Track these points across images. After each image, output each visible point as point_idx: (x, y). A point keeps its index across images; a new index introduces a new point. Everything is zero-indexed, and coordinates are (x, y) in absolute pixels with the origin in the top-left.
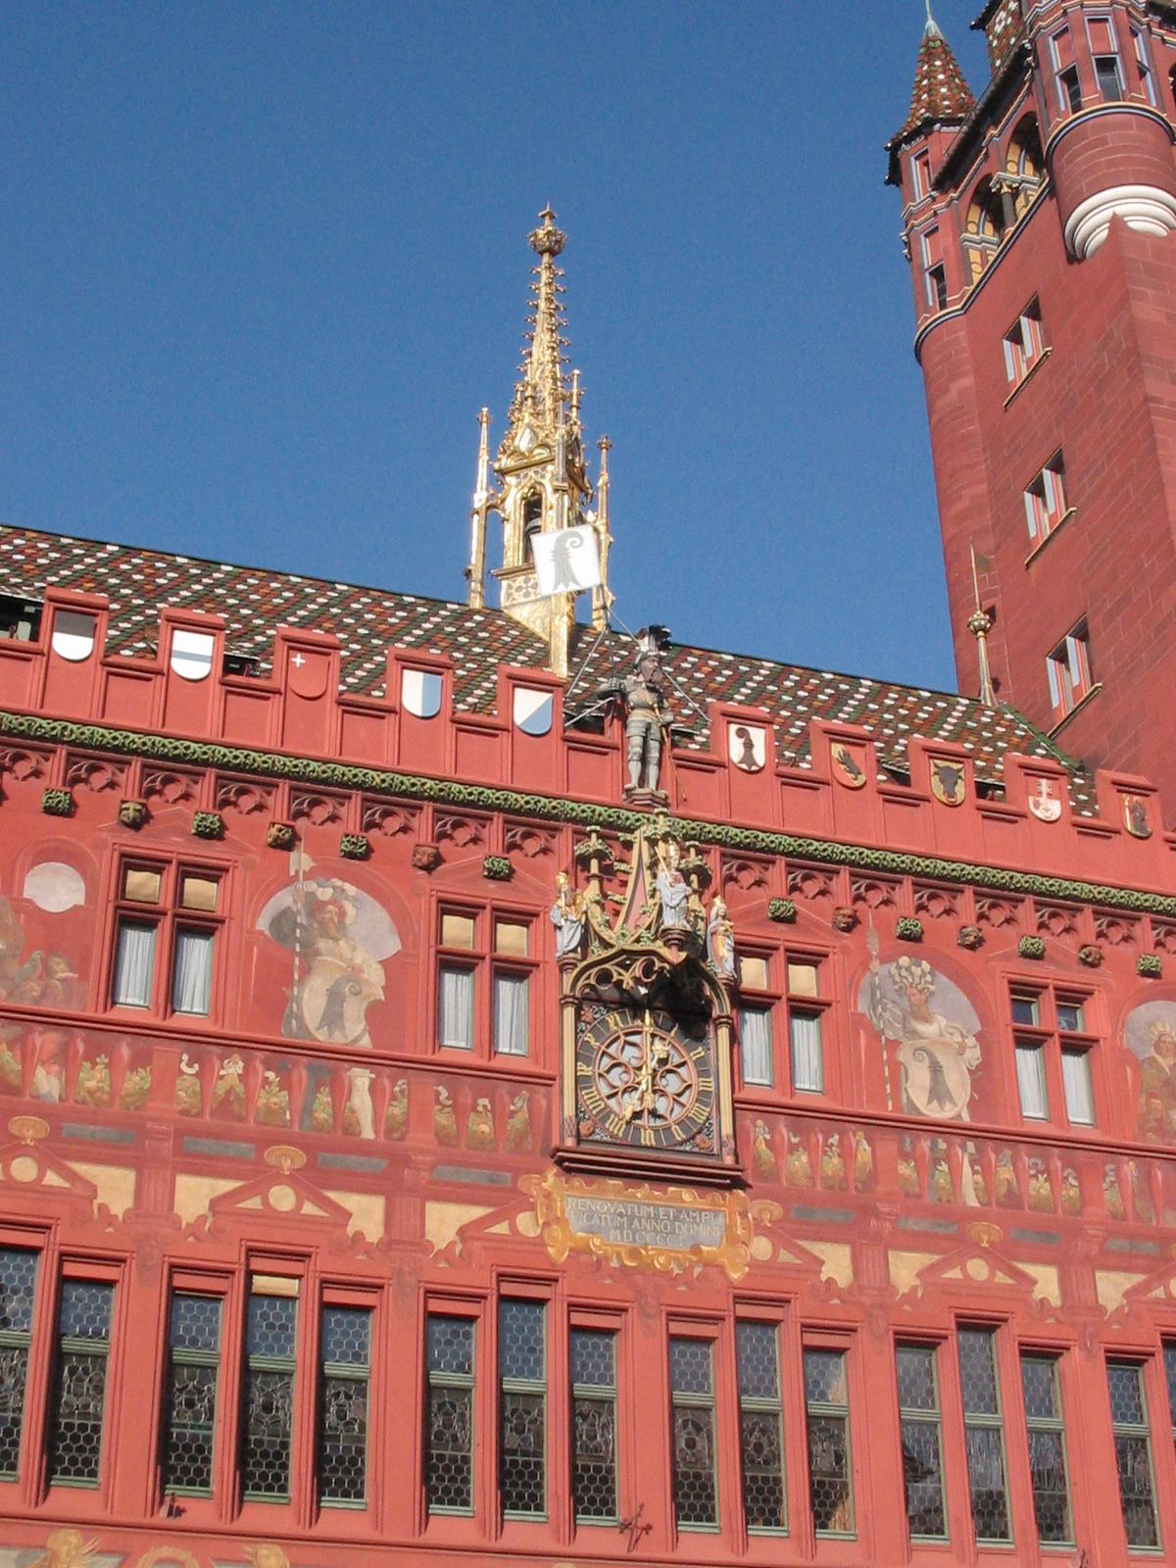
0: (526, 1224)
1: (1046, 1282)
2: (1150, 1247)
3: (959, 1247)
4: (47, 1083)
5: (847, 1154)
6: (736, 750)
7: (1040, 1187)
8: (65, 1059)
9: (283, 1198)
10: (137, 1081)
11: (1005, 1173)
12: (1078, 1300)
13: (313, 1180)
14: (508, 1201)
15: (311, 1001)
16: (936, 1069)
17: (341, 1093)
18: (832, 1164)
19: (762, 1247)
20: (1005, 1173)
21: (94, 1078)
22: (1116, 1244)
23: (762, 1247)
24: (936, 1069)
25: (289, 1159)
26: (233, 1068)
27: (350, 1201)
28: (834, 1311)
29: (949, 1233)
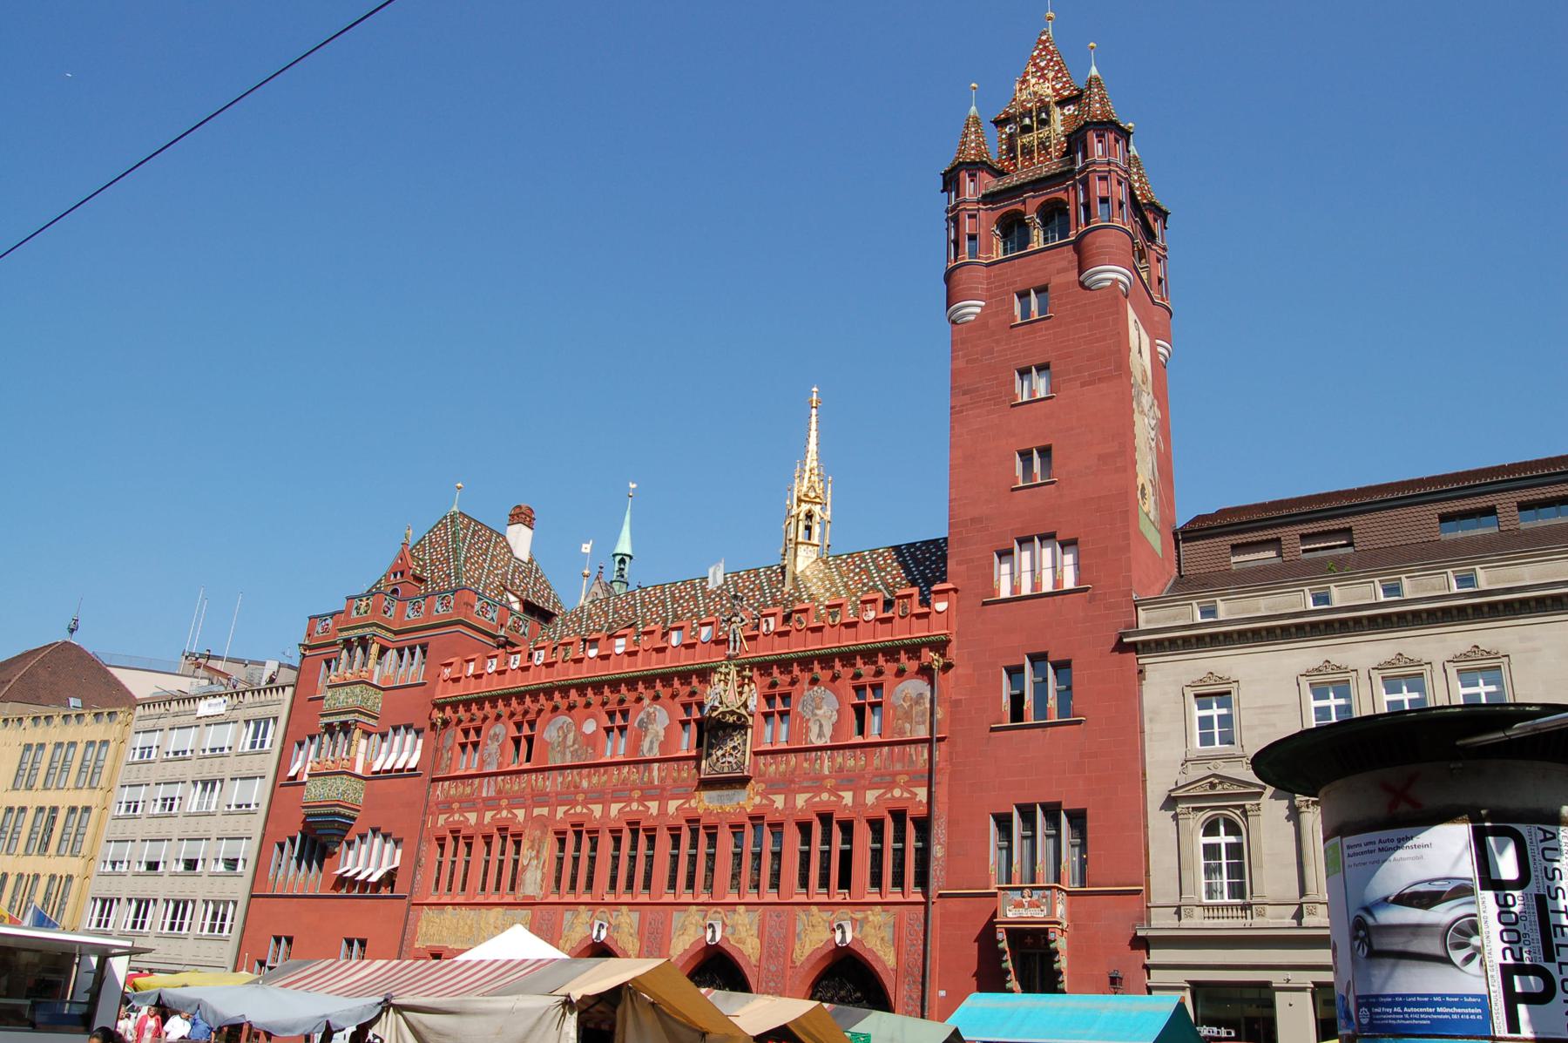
0: (693, 803)
1: (848, 797)
2: (888, 779)
3: (819, 789)
4: (585, 784)
5: (787, 763)
6: (764, 628)
7: (851, 763)
8: (589, 776)
9: (635, 806)
10: (604, 778)
11: (840, 760)
12: (858, 802)
13: (642, 800)
14: (688, 797)
15: (646, 745)
16: (821, 726)
17: (651, 772)
18: (783, 767)
19: (757, 799)
20: (840, 760)
21: (595, 780)
22: (877, 779)
23: (757, 799)
24: (821, 726)
25: (637, 794)
26: (626, 769)
27: (649, 804)
28: (777, 818)
29: (817, 783)
